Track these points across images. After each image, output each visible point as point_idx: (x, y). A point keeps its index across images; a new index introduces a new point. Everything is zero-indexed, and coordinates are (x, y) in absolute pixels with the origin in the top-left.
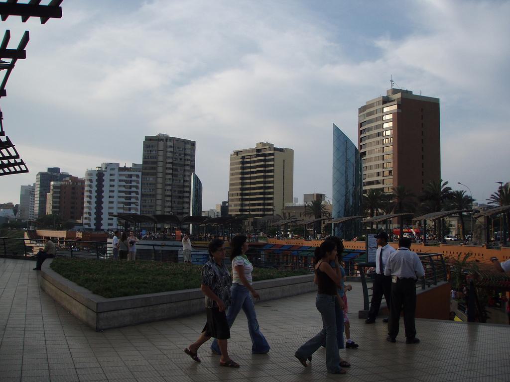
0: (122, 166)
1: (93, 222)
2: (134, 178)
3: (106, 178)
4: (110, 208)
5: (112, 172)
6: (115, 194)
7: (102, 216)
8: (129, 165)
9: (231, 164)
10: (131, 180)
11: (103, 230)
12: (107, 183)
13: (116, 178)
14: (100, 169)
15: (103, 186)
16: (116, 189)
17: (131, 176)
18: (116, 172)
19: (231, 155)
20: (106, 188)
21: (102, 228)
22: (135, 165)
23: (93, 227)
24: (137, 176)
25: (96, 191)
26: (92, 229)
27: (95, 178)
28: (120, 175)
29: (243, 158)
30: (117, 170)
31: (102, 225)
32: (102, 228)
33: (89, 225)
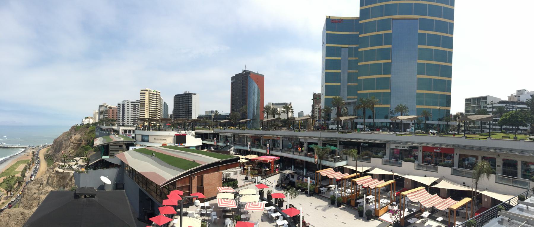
3: (126, 106)
5: (128, 103)
6: (130, 112)
8: (134, 101)
9: (174, 104)
12: (126, 108)
13: (130, 105)
17: (135, 105)
18: (130, 104)
19: (174, 96)
20: (126, 110)
22: (137, 101)
24: (138, 105)
27: (121, 106)
28: (131, 105)
29: (179, 97)
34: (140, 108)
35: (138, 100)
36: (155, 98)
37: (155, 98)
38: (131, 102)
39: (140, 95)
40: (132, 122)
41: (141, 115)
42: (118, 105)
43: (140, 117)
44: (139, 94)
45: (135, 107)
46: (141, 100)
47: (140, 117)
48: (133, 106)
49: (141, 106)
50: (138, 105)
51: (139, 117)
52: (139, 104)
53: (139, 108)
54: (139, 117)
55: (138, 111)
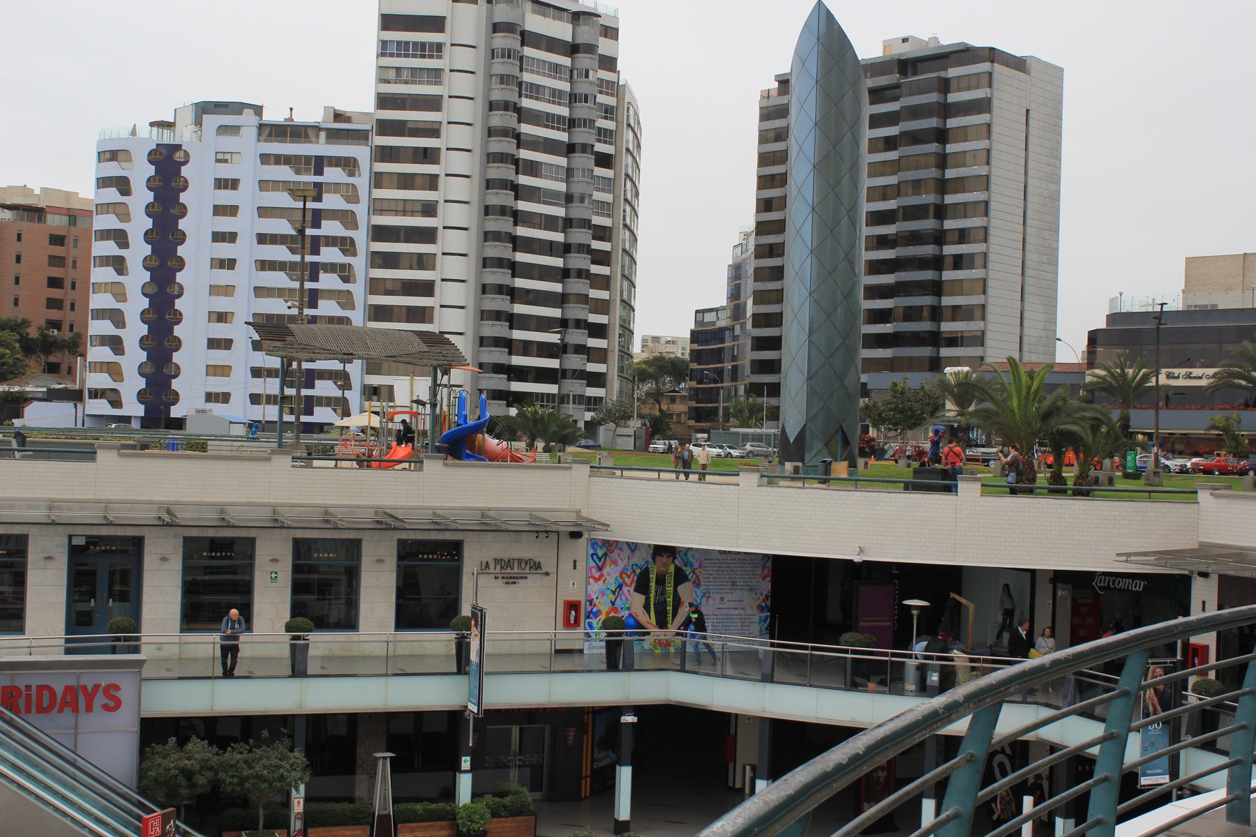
1: (132, 385)
2: (331, 201)
6: (245, 251)
10: (318, 186)
14: (167, 138)
16: (246, 224)
17: (319, 164)
18: (248, 144)
21: (175, 412)
23: (136, 410)
24: (349, 164)
25: (148, 237)
26: (127, 419)
27: (141, 172)
28: (265, 159)
30: (249, 133)
31: (175, 398)
32: (175, 412)
34: (378, 207)
35: (344, 107)
36: (556, 96)
37: (556, 96)
39: (373, 48)
41: (375, 286)
43: (379, 313)
44: (371, 33)
45: (318, 191)
46: (384, 101)
47: (379, 313)
48: (285, 173)
49: (378, 180)
50: (349, 164)
51: (357, 317)
52: (362, 153)
53: (361, 210)
54: (357, 317)
55: (347, 246)
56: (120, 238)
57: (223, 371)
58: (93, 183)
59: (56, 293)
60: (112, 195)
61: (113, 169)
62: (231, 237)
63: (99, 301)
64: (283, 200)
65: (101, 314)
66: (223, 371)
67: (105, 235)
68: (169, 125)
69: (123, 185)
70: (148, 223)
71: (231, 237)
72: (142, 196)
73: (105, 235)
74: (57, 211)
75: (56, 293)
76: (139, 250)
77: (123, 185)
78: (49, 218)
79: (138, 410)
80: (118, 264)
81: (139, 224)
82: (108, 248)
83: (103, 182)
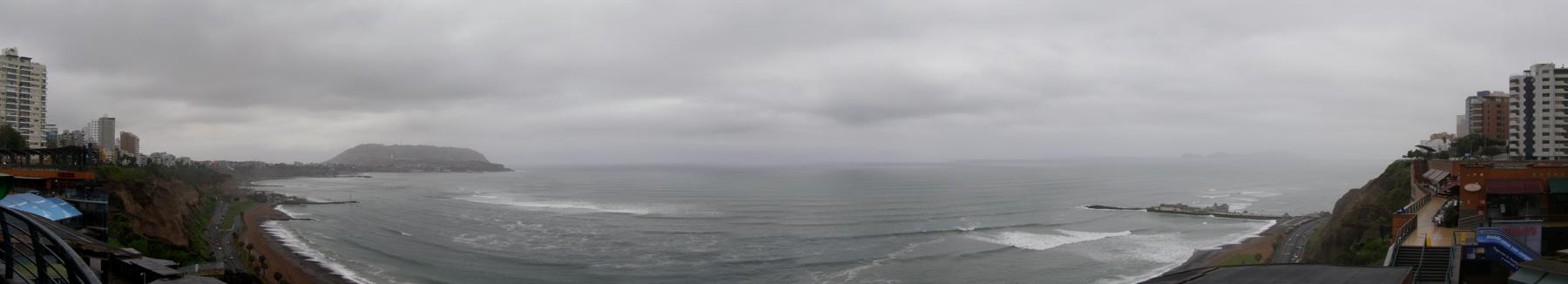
0: (1558, 66)
1: (1522, 147)
3: (1538, 84)
4: (1545, 126)
5: (1546, 76)
7: (1534, 123)
11: (1536, 158)
12: (1538, 91)
13: (1551, 83)
14: (1528, 75)
15: (1534, 88)
18: (1551, 75)
20: (1538, 99)
27: (1522, 85)
28: (1557, 79)
30: (1552, 72)
31: (1534, 150)
32: (1534, 155)
33: (1516, 150)
38: (1557, 71)
40: (1561, 142)
42: (1511, 81)
56: (1517, 104)
57: (1547, 142)
58: (1508, 81)
59: (1499, 121)
60: (1514, 92)
61: (1514, 85)
62: (1548, 87)
63: (1512, 123)
64: (1563, 107)
65: (1513, 127)
66: (1547, 142)
67: (1513, 104)
68: (1529, 71)
69: (1517, 89)
70: (1524, 123)
71: (1548, 103)
72: (1523, 92)
73: (1513, 104)
74: (1498, 98)
75: (1499, 121)
76: (1522, 108)
77: (1517, 89)
78: (1497, 100)
79: (1524, 154)
80: (1517, 112)
81: (1523, 100)
82: (1514, 108)
83: (1511, 89)
